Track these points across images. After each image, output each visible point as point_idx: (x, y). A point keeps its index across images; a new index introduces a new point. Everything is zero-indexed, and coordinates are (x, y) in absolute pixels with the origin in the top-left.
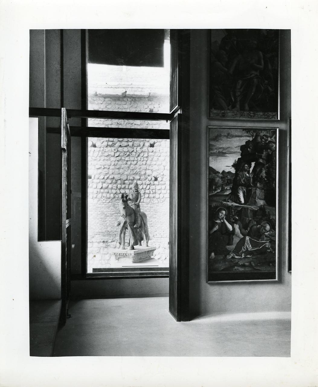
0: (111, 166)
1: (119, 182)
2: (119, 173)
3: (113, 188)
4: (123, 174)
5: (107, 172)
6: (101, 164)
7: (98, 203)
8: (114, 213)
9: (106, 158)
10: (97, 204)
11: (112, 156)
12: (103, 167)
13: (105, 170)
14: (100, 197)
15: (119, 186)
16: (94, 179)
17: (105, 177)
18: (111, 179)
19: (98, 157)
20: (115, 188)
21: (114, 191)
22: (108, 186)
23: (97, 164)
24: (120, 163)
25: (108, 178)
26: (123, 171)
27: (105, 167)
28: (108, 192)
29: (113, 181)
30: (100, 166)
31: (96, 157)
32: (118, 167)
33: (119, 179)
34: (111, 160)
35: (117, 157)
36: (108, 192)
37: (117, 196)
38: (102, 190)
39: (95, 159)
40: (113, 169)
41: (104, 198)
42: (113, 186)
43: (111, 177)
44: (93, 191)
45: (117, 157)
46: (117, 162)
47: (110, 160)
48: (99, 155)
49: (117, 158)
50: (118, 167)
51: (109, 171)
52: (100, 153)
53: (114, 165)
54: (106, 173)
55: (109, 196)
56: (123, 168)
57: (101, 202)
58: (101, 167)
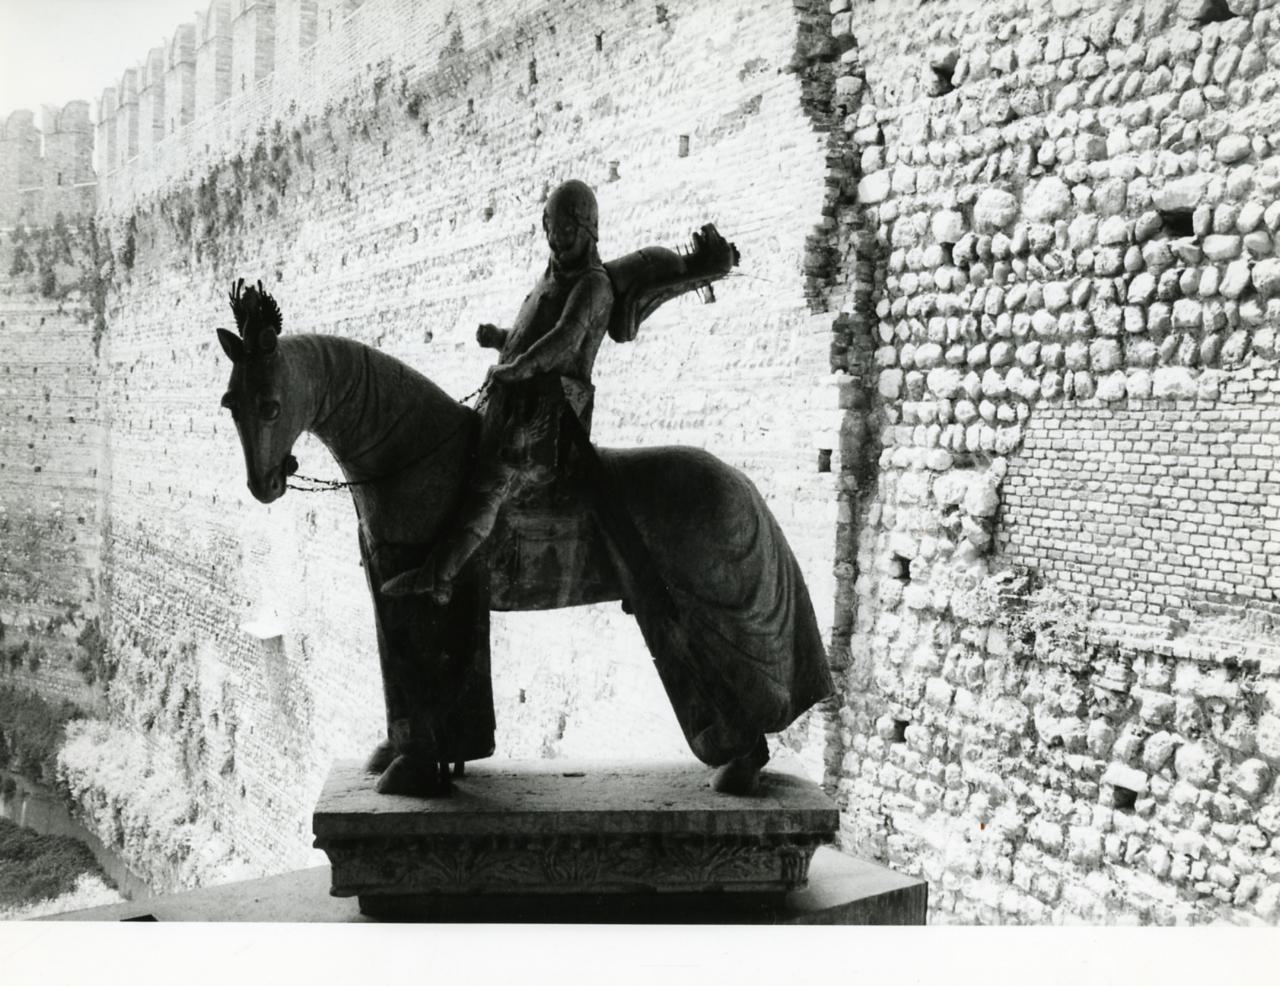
6: (1250, 122)
7: (1224, 397)
10: (1219, 406)
12: (1259, 145)
14: (1235, 358)
16: (1209, 230)
19: (1236, 83)
23: (1226, 133)
31: (1228, 81)
38: (1249, 310)
41: (1257, 362)
44: (1201, 315)
48: (1243, 67)
52: (1252, 46)
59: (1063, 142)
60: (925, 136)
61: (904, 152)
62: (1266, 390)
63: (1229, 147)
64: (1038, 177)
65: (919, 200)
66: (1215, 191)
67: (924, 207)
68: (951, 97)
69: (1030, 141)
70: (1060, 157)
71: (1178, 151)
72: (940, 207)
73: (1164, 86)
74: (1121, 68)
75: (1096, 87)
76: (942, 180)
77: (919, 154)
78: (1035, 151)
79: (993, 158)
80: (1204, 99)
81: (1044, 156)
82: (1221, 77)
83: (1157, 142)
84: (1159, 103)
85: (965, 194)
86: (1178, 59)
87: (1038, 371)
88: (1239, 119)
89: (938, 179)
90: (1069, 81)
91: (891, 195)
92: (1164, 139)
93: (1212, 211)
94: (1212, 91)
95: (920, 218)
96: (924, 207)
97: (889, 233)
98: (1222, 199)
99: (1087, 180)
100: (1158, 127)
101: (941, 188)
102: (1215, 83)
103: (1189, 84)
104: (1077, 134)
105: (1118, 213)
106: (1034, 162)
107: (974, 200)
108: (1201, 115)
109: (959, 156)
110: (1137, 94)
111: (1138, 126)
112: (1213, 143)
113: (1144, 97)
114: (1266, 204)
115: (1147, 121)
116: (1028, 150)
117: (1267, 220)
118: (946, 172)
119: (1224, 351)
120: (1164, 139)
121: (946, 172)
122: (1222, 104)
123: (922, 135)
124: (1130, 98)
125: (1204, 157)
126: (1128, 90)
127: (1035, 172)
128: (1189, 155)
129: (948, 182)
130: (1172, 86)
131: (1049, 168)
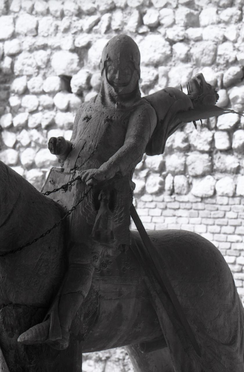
59: (164, 11)
61: (28, 5)
64: (144, 34)
65: (40, 41)
67: (44, 47)
69: (138, 8)
70: (162, 22)
72: (59, 48)
76: (61, 28)
78: (142, 15)
79: (106, 17)
81: (150, 18)
85: (82, 40)
89: (57, 27)
91: (14, 36)
95: (41, 56)
96: (44, 47)
97: (12, 65)
99: (185, 40)
101: (60, 34)
104: (177, 7)
105: (210, 65)
106: (141, 23)
107: (88, 46)
109: (76, 12)
111: (225, 7)
116: (136, 15)
118: (64, 24)
121: (64, 24)
127: (141, 30)
129: (66, 30)
131: (154, 28)
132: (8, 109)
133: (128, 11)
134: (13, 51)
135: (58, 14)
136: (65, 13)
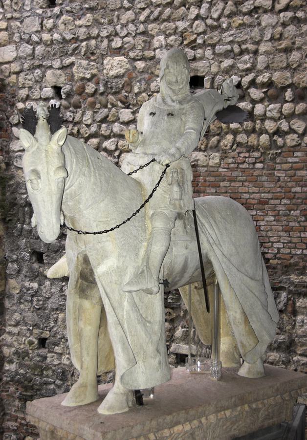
0: (262, 44)
1: (289, 94)
2: (288, 67)
3: (268, 114)
4: (299, 66)
5: (249, 65)
6: (231, 38)
7: (222, 166)
8: (270, 196)
9: (247, 19)
11: (266, 11)
12: (236, 49)
13: (246, 57)
14: (229, 147)
15: (287, 108)
17: (243, 79)
18: (263, 85)
19: (223, 19)
20: (275, 114)
21: (270, 125)
22: (253, 108)
24: (291, 29)
25: (253, 83)
26: (299, 55)
27: (244, 47)
28: (253, 131)
29: (269, 93)
30: (229, 47)
32: (283, 46)
33: (287, 83)
34: (263, 24)
35: (280, 11)
36: (253, 131)
37: (280, 141)
39: (215, 23)
40: (267, 53)
42: (267, 109)
43: (263, 78)
45: (280, 11)
46: (280, 29)
47: (259, 24)
48: (227, 12)
49: (282, 15)
50: (284, 44)
51: (256, 59)
53: (272, 39)
54: (245, 67)
55: (255, 143)
56: (299, 48)
57: (230, 160)
58: (232, 51)
60: (39, 29)
62: (244, 162)
63: (220, 49)
66: (214, 69)
67: (40, 66)
68: (56, 10)
69: (107, 37)
71: (193, 48)
73: (183, 18)
74: (159, 6)
75: (146, 13)
77: (35, 38)
80: (206, 25)
82: (215, 16)
83: (182, 43)
84: (182, 25)
85: (68, 61)
86: (192, 4)
87: (117, 154)
88: (227, 37)
90: (128, 9)
92: (185, 42)
93: (213, 79)
94: (209, 22)
95: (38, 72)
96: (40, 66)
98: (217, 74)
99: (143, 59)
100: (181, 36)
102: (211, 18)
103: (198, 17)
108: (204, 33)
110: (168, 19)
111: (170, 35)
112: (213, 46)
113: (174, 20)
114: (242, 77)
115: (175, 33)
117: (243, 84)
119: (222, 144)
120: (185, 42)
122: (213, 28)
123: (37, 27)
124: (164, 21)
125: (208, 53)
126: (164, 16)
128: (199, 51)
130: (189, 17)
132: (16, 111)
133: (99, 39)
134: (17, 69)
135: (49, 42)
136: (54, 42)
